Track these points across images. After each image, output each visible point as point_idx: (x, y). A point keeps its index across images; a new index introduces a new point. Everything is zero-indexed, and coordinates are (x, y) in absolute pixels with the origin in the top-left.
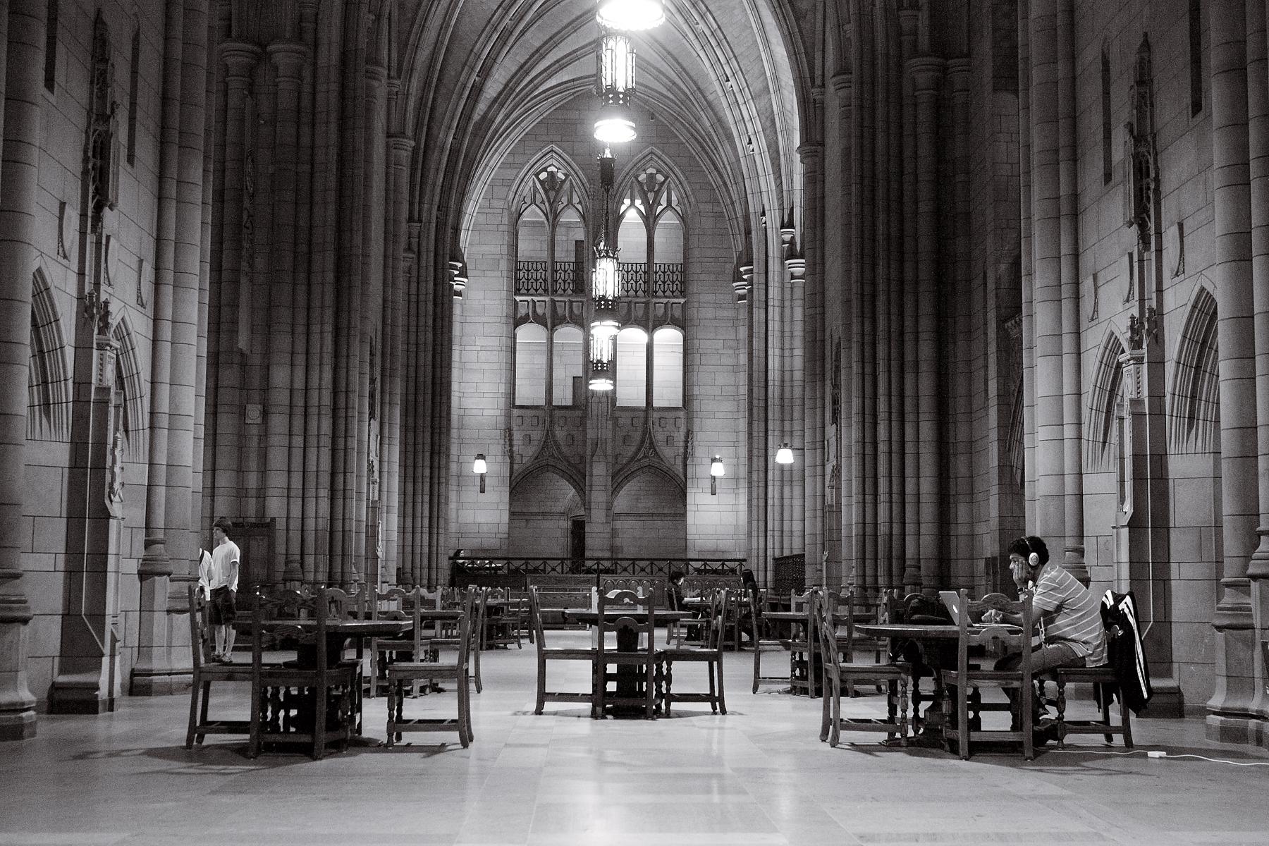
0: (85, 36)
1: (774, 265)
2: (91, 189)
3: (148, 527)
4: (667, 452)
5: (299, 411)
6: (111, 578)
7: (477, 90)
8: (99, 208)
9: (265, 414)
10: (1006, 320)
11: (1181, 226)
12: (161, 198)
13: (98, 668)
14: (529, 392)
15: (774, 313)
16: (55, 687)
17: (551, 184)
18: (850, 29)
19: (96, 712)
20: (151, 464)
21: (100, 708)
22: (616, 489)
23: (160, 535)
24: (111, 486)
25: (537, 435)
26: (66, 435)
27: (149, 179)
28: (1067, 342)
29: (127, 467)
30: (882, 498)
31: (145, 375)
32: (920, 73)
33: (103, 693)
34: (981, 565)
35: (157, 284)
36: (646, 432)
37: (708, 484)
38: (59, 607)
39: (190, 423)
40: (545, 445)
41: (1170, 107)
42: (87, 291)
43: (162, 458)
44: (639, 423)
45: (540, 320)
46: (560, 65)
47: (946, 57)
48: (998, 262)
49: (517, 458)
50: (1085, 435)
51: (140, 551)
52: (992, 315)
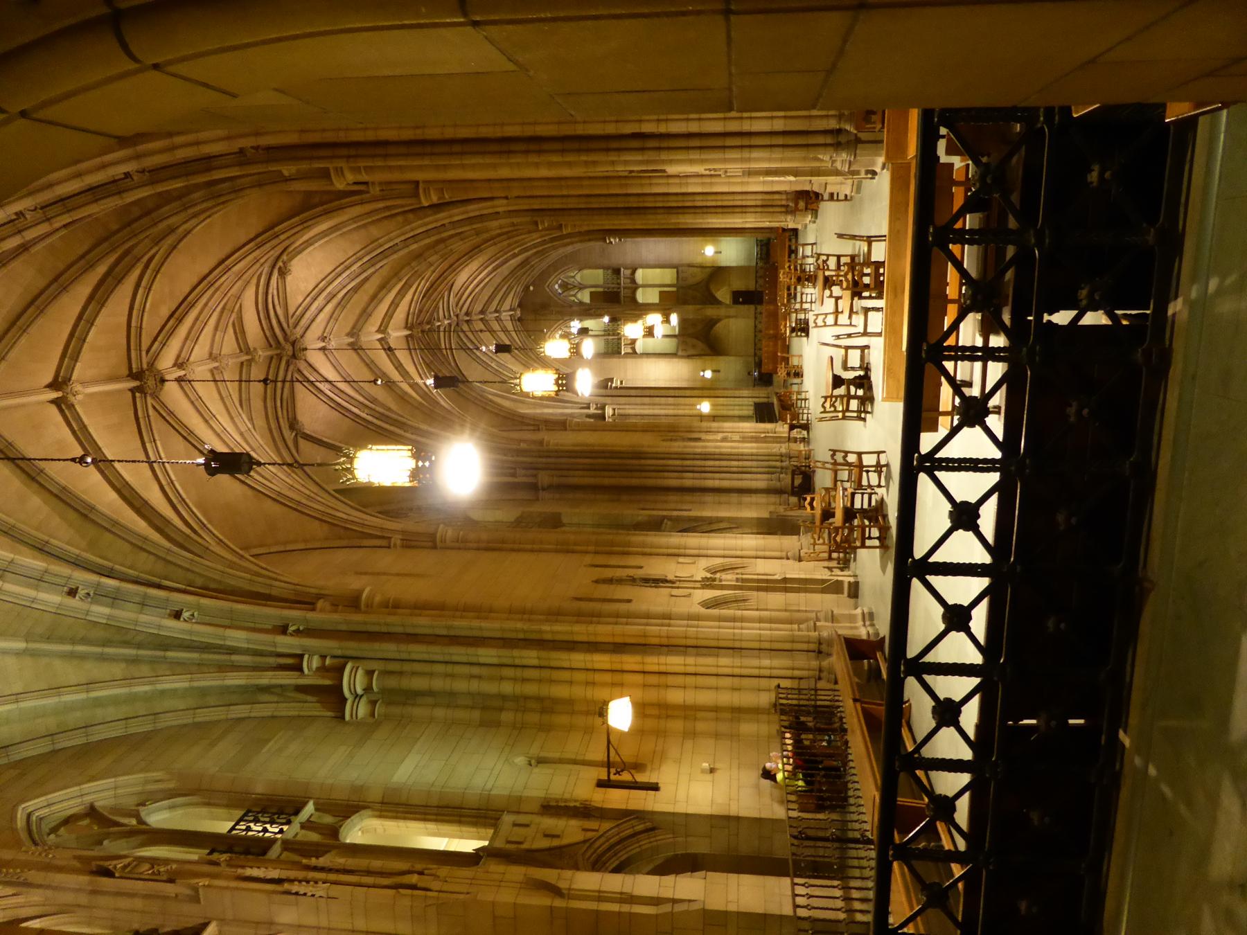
3: (781, 558)
8: (667, 581)
12: (651, 554)
13: (841, 582)
16: (849, 596)
33: (852, 580)
36: (690, 287)
40: (697, 338)
51: (791, 562)
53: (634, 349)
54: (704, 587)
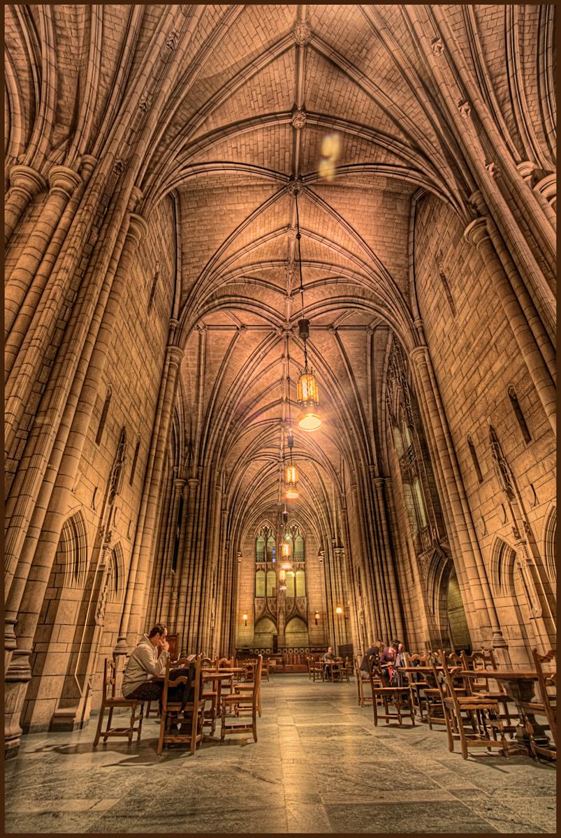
0: (117, 433)
1: (330, 551)
2: (111, 486)
3: (120, 633)
4: (302, 611)
5: (189, 594)
6: (92, 655)
7: (246, 503)
8: (113, 494)
9: (179, 596)
10: (419, 554)
11: (532, 485)
13: (77, 705)
15: (332, 565)
18: (355, 472)
19: (71, 730)
20: (125, 604)
21: (75, 727)
22: (286, 624)
23: (124, 636)
24: (99, 610)
25: (262, 606)
26: (83, 586)
27: (138, 493)
28: (474, 546)
29: (111, 605)
30: (383, 620)
31: (127, 566)
32: (377, 483)
33: (77, 719)
34: (423, 645)
35: (137, 532)
37: (314, 621)
38: (65, 671)
39: (143, 587)
41: (509, 448)
42: (102, 524)
43: (129, 602)
44: (293, 601)
45: (263, 570)
46: (268, 497)
47: (385, 478)
48: (412, 536)
50: (490, 581)
52: (413, 553)
53: (259, 570)
54: (100, 532)
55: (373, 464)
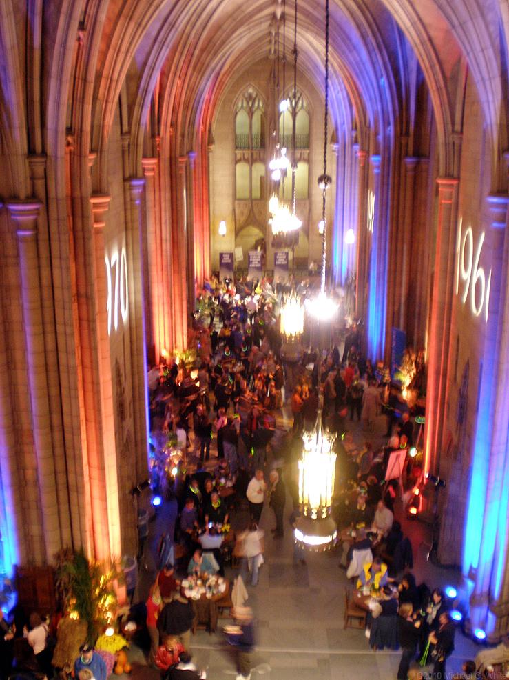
14: (243, 192)
17: (250, 98)
25: (246, 211)
45: (246, 161)
49: (237, 222)
55: (407, 134)
